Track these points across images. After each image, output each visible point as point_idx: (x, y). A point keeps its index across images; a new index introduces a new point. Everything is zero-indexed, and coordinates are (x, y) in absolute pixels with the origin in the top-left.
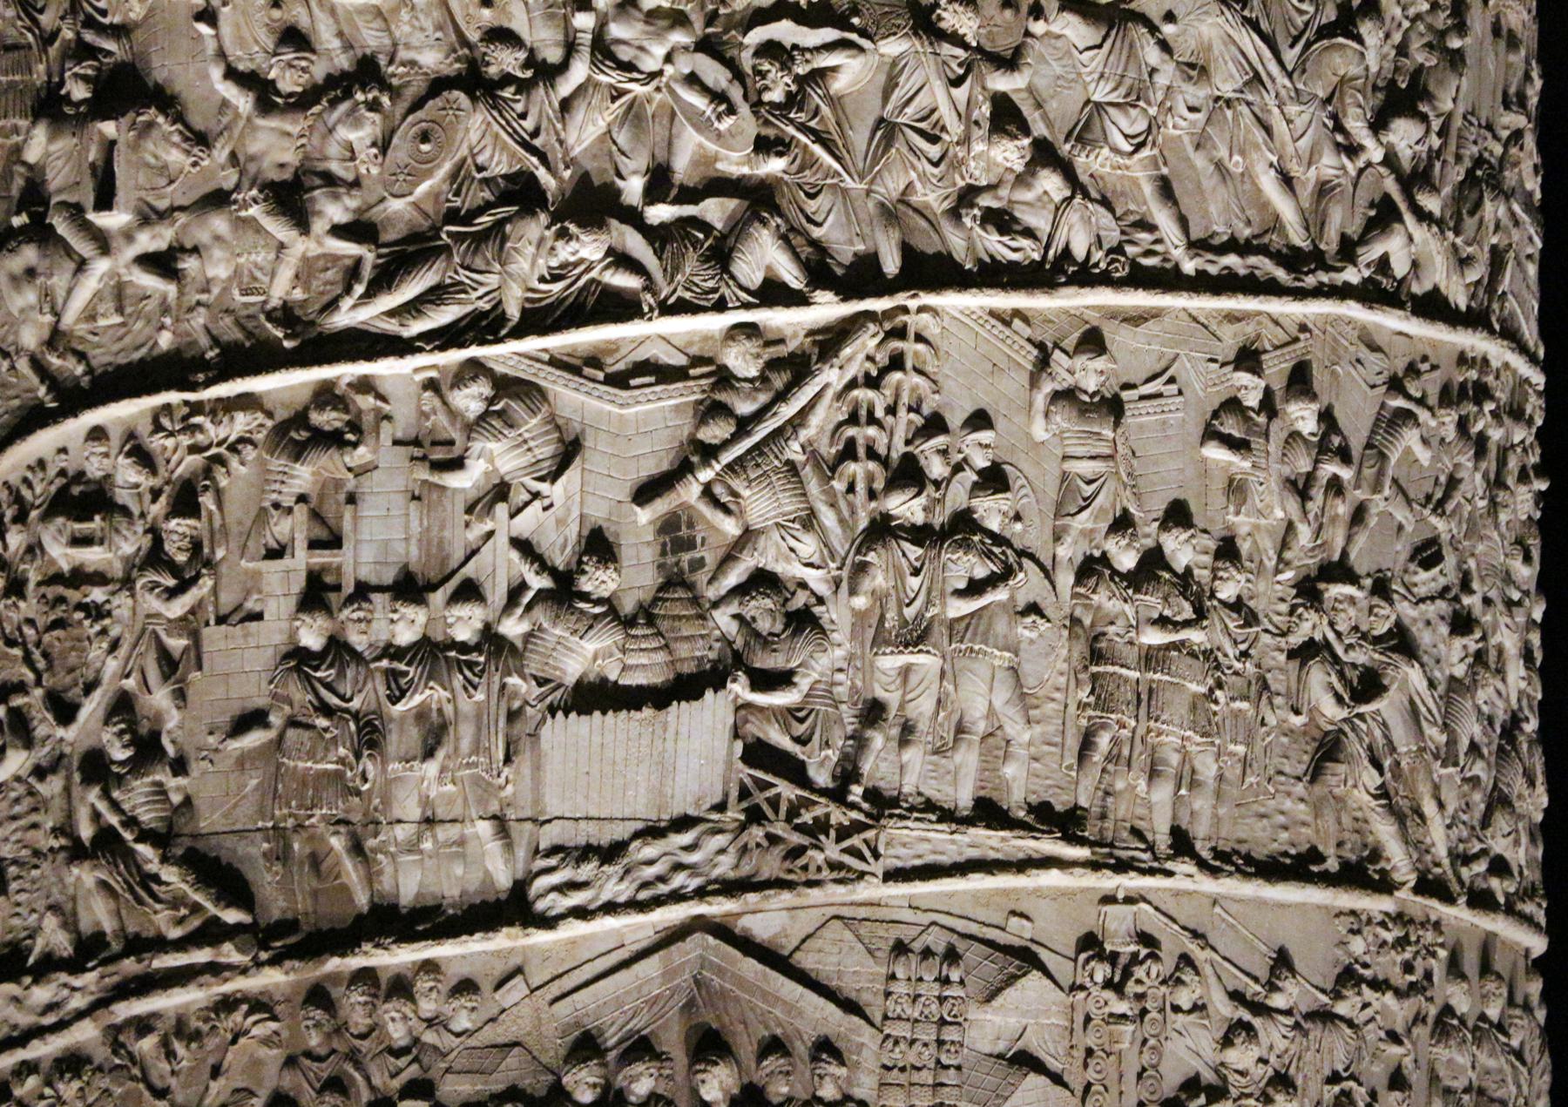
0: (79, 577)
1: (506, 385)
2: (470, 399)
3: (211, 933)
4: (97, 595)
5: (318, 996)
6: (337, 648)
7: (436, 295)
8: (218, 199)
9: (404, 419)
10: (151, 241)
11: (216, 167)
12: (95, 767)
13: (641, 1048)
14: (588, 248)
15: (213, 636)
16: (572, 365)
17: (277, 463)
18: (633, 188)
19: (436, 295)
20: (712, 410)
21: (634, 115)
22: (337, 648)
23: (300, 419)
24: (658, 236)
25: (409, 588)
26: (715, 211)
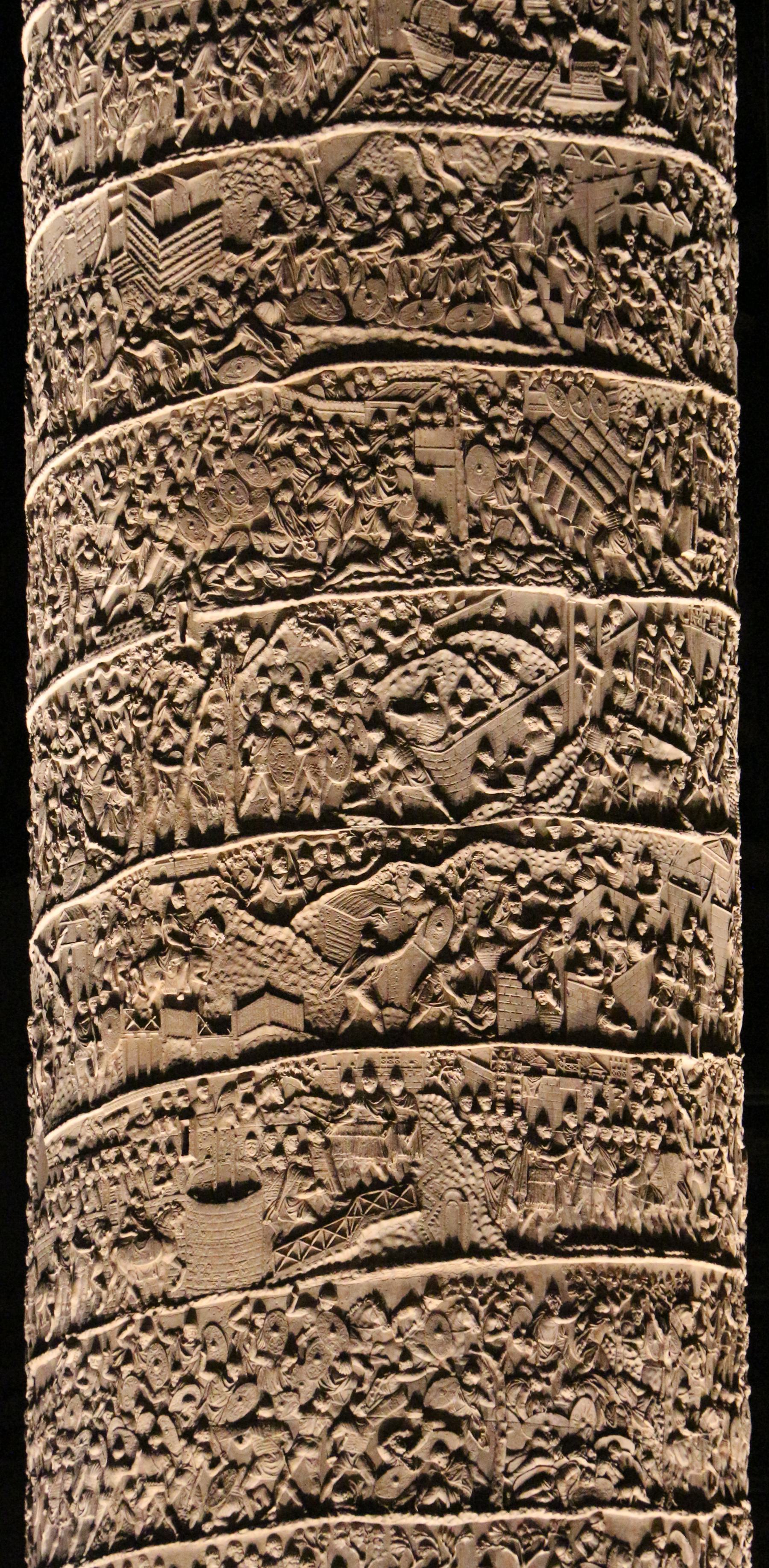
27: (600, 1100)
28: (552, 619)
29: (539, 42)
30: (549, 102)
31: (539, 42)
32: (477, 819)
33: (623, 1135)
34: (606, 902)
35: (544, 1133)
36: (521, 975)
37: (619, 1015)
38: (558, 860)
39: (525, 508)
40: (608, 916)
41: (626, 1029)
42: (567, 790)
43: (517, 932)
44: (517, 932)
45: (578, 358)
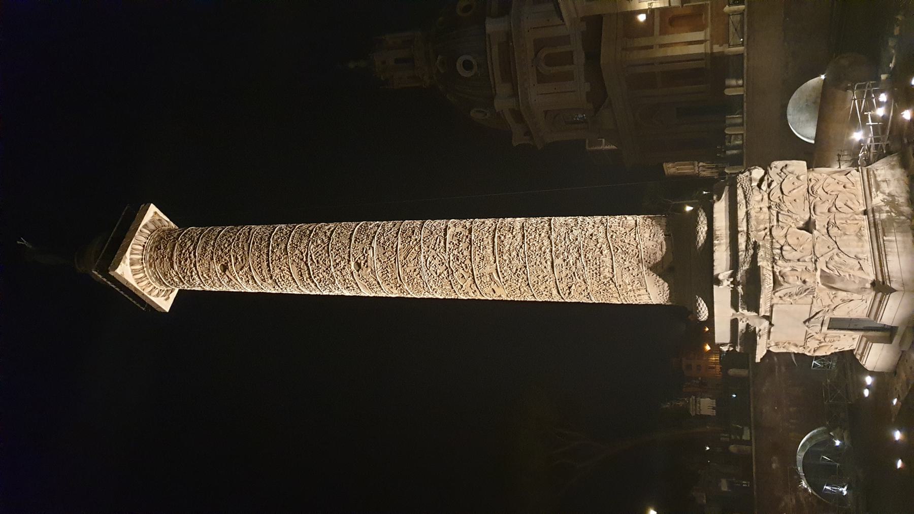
12: (626, 235)
27: (478, 251)
28: (425, 256)
29: (366, 258)
30: (371, 256)
31: (366, 258)
32: (448, 266)
33: (482, 247)
34: (455, 249)
35: (482, 258)
36: (464, 261)
37: (468, 248)
38: (451, 256)
39: (413, 260)
40: (457, 249)
41: (469, 247)
42: (443, 255)
43: (460, 261)
44: (460, 261)
45: (397, 253)
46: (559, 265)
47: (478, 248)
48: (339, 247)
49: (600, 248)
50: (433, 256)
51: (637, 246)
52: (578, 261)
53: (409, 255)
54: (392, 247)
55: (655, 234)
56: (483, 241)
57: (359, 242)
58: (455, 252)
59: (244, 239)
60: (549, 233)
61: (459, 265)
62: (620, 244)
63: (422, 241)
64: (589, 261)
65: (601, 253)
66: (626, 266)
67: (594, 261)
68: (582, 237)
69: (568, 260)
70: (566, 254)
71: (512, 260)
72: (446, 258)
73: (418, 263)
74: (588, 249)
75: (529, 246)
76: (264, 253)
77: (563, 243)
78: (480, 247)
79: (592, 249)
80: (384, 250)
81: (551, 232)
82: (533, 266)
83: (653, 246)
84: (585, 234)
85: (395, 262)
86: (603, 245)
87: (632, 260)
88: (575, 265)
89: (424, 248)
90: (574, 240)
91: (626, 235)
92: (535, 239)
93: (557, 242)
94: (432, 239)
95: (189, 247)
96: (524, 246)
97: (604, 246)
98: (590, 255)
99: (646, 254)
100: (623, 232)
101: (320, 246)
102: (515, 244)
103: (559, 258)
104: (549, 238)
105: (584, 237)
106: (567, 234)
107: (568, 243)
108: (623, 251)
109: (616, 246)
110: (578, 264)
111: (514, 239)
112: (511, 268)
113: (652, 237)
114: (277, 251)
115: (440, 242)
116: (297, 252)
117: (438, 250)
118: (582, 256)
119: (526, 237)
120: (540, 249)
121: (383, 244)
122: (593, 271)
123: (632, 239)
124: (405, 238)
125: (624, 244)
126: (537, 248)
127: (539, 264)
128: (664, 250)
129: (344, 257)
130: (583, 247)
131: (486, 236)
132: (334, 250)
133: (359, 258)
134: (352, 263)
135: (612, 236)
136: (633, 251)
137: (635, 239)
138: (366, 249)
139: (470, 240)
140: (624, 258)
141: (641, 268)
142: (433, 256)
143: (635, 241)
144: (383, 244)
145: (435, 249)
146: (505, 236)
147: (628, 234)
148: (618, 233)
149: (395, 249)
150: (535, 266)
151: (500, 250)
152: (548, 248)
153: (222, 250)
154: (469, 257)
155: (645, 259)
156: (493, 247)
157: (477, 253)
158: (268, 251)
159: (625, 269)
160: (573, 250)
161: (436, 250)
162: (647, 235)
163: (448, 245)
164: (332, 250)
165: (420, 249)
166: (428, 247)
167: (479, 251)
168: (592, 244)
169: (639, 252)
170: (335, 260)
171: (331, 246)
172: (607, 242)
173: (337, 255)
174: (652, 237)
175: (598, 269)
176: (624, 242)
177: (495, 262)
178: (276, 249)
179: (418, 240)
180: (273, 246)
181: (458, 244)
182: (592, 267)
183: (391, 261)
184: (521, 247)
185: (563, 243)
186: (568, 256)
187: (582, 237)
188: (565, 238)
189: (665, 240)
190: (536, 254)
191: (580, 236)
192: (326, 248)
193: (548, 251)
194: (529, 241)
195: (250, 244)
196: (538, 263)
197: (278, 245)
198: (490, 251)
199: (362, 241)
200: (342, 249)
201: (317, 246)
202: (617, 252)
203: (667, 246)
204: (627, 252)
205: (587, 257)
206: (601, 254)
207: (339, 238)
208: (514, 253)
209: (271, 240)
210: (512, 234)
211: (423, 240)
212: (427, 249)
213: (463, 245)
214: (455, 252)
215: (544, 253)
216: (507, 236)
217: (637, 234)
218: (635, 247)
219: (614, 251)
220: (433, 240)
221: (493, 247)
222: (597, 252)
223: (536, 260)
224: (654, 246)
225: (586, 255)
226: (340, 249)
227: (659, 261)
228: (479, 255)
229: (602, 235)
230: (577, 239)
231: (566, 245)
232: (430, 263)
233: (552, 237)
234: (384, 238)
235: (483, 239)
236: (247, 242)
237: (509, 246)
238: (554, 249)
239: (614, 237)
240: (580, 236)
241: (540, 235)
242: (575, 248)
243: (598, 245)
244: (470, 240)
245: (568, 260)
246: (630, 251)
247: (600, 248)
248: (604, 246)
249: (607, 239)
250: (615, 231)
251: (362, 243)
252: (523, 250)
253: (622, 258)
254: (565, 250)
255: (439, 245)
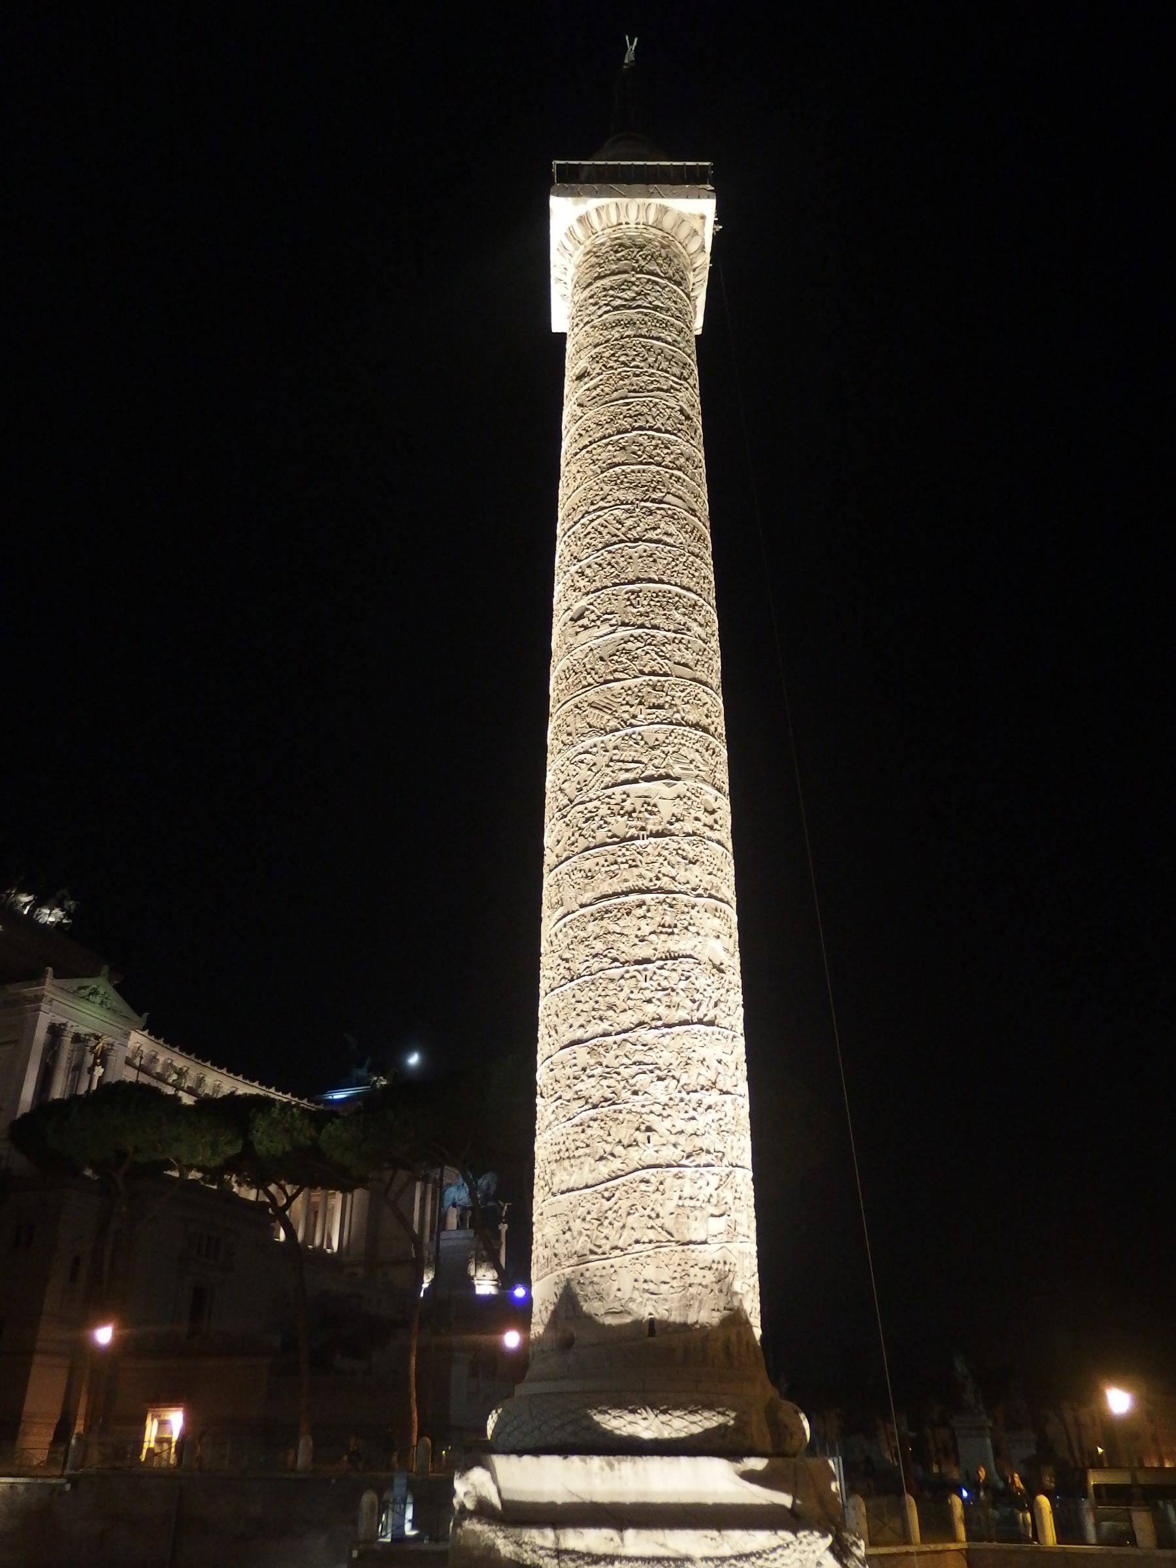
0: (645, 1191)
1: (701, 1174)
2: (698, 1175)
3: (669, 1241)
4: (649, 1194)
5: (683, 1251)
6: (683, 1206)
7: (694, 1161)
8: (664, 1145)
9: (689, 1177)
10: (656, 1149)
11: (663, 1141)
12: (650, 1217)
13: (719, 1263)
14: (709, 1157)
15: (667, 1202)
16: (709, 1172)
17: (675, 1180)
18: (712, 1151)
19: (694, 1161)
20: (721, 1180)
21: (712, 1141)
22: (683, 1206)
23: (677, 1175)
24: (716, 1157)
25: (691, 1198)
26: (720, 1155)
27: (606, 861)
28: (595, 746)
30: (595, 635)
31: (593, 624)
34: (609, 809)
35: (589, 874)
38: (597, 803)
39: (588, 724)
40: (609, 812)
41: (615, 839)
42: (597, 784)
43: (584, 825)
44: (584, 825)
45: (602, 684)
46: (575, 1058)
47: (611, 858)
48: (617, 563)
49: (613, 1155)
50: (594, 764)
51: (616, 1248)
52: (582, 1102)
53: (597, 711)
54: (615, 671)
55: (653, 1294)
56: (630, 866)
57: (628, 599)
58: (604, 810)
59: (637, 385)
60: (654, 1023)
61: (577, 826)
62: (625, 1204)
63: (630, 730)
64: (583, 1131)
65: (601, 1158)
66: (571, 1224)
67: (582, 1141)
68: (643, 1106)
69: (584, 1077)
70: (599, 1070)
71: (586, 943)
72: (591, 795)
73: (582, 735)
74: (611, 1123)
75: (617, 978)
76: (607, 429)
77: (626, 1061)
78: (616, 862)
79: (609, 1135)
80: (610, 656)
81: (657, 1028)
82: (574, 996)
83: (619, 1290)
84: (652, 1112)
85: (584, 687)
86: (620, 1160)
87: (584, 1238)
88: (576, 1096)
89: (613, 739)
90: (635, 1085)
91: (650, 1217)
92: (636, 991)
93: (629, 1045)
94: (636, 751)
95: (619, 298)
96: (616, 967)
97: (616, 1164)
98: (595, 1130)
99: (599, 1273)
100: (659, 1209)
101: (620, 526)
102: (622, 945)
103: (588, 1056)
104: (641, 1024)
105: (644, 1110)
106: (651, 1067)
107: (626, 1073)
108: (606, 1212)
109: (617, 1194)
110: (575, 1105)
111: (636, 941)
112: (571, 947)
113: (646, 1286)
114: (609, 451)
115: (627, 770)
116: (607, 488)
117: (608, 770)
118: (593, 1113)
119: (640, 967)
120: (611, 1007)
121: (624, 649)
122: (564, 1143)
123: (636, 1235)
124: (640, 691)
125: (624, 1215)
126: (613, 1000)
127: (578, 1011)
128: (609, 1320)
129: (594, 581)
130: (615, 1112)
131: (644, 872)
132: (609, 556)
133: (593, 612)
134: (584, 602)
135: (647, 1182)
136: (607, 1238)
137: (637, 1242)
138: (611, 620)
139: (632, 838)
140: (588, 1218)
141: (568, 1263)
142: (594, 764)
143: (631, 1241)
144: (624, 649)
145: (611, 764)
146: (644, 917)
147: (651, 1223)
148: (658, 1195)
149: (610, 677)
150: (573, 1001)
151: (607, 912)
152: (611, 1025)
153: (613, 355)
154: (592, 845)
155: (587, 1270)
156: (616, 895)
157: (601, 860)
158: (610, 436)
159: (568, 1222)
160: (608, 1087)
161: (608, 766)
162: (649, 1272)
163: (618, 790)
164: (610, 552)
165: (612, 731)
166: (616, 748)
167: (606, 864)
168: (624, 1133)
169: (604, 1253)
170: (589, 567)
171: (620, 549)
172: (627, 1170)
173: (600, 565)
174: (646, 1286)
175: (567, 1154)
176: (629, 1214)
177: (582, 906)
178: (613, 449)
179: (633, 721)
180: (621, 441)
181: (622, 812)
182: (571, 1138)
183: (585, 677)
184: (615, 960)
185: (626, 1061)
186: (593, 1076)
187: (643, 1106)
188: (640, 1063)
189: (637, 1323)
190: (600, 999)
191: (646, 1100)
192: (615, 539)
193: (604, 1026)
194: (631, 977)
195: (627, 398)
196: (580, 1006)
197: (623, 448)
198: (606, 888)
199: (631, 604)
200: (613, 570)
201: (619, 522)
202: (603, 1197)
203: (621, 1327)
204: (601, 1224)
205: (591, 1123)
206: (597, 1158)
207: (640, 557)
208: (599, 946)
209: (635, 433)
210: (651, 933)
211: (634, 733)
212: (610, 746)
213: (619, 825)
214: (604, 810)
215: (601, 1019)
216: (643, 922)
217: (652, 1245)
218: (615, 1243)
219: (606, 1190)
220: (633, 754)
221: (616, 895)
222: (601, 1148)
223: (587, 1002)
224: (619, 1294)
225: (595, 1120)
226: (613, 567)
227: (581, 1308)
228: (597, 864)
229: (648, 1154)
230: (635, 1093)
231: (621, 1069)
232: (582, 762)
233: (640, 1031)
234: (637, 649)
235: (636, 866)
236: (630, 392)
237: (618, 930)
238: (609, 1040)
239: (643, 1186)
240: (646, 1100)
241: (649, 1001)
242: (613, 1092)
243: (620, 1148)
244: (632, 838)
245: (584, 1077)
246: (606, 1232)
247: (613, 1155)
248: (616, 1164)
249: (637, 1170)
250: (661, 1188)
251: (626, 606)
252: (607, 966)
253: (589, 1213)
254: (607, 1067)
255: (621, 769)
